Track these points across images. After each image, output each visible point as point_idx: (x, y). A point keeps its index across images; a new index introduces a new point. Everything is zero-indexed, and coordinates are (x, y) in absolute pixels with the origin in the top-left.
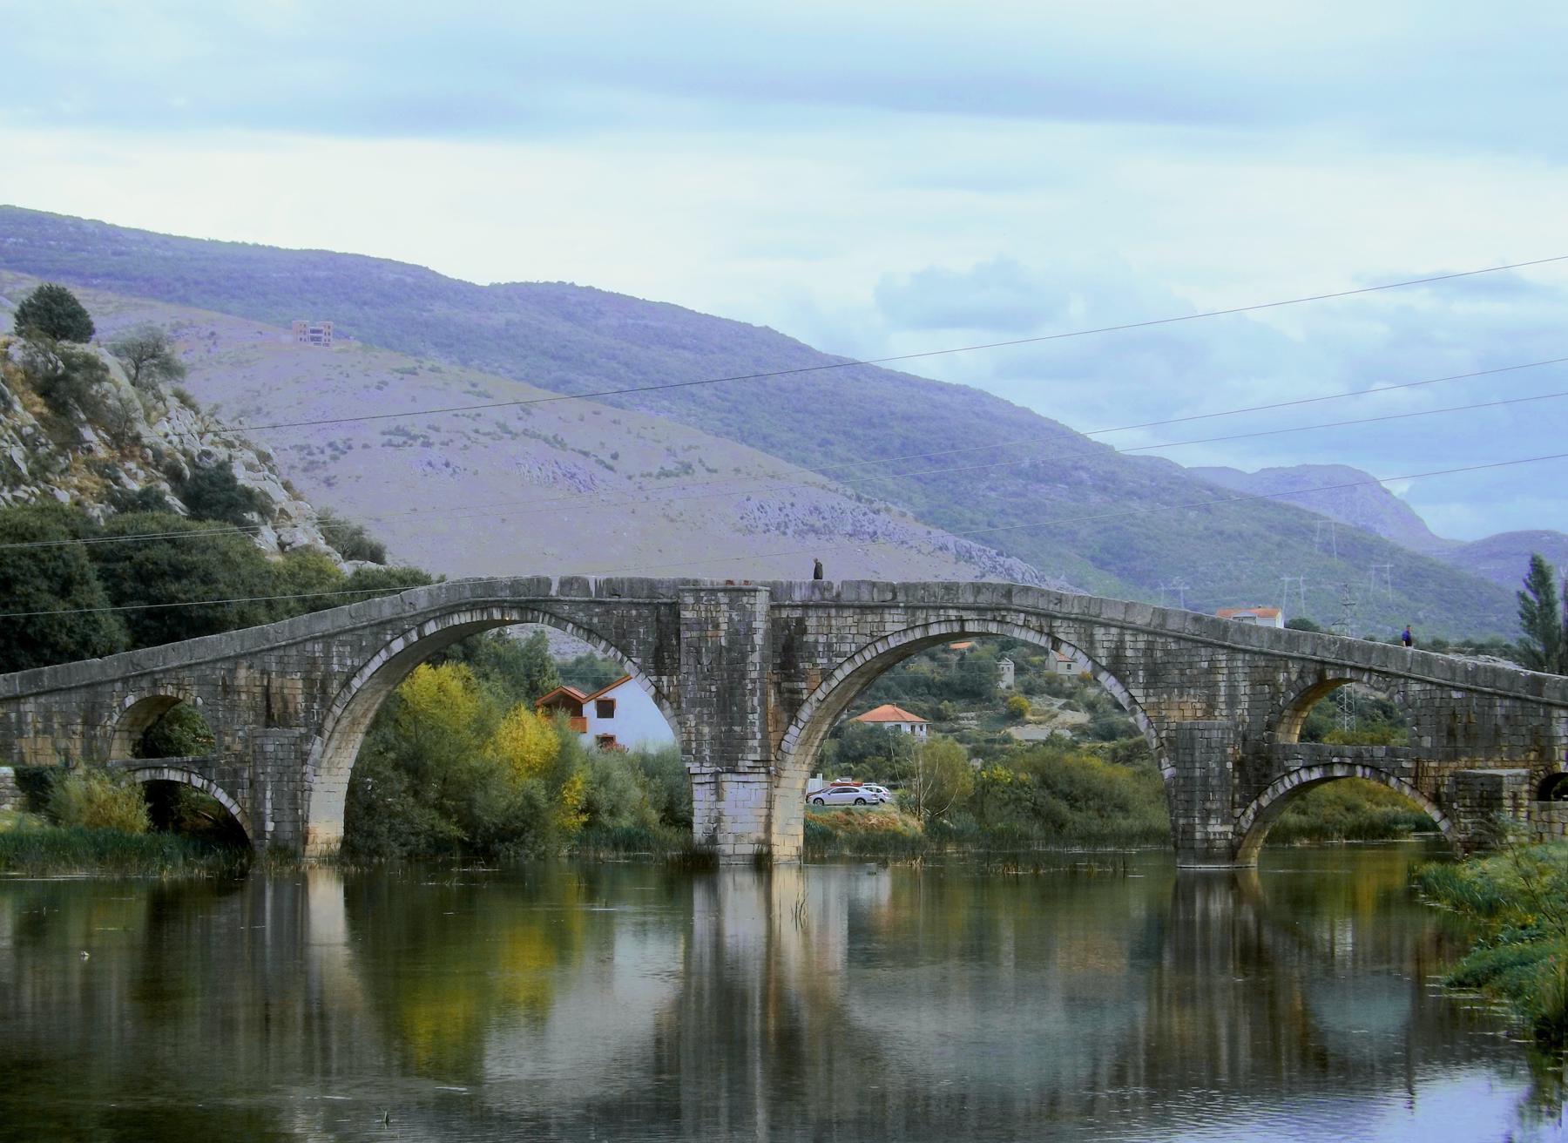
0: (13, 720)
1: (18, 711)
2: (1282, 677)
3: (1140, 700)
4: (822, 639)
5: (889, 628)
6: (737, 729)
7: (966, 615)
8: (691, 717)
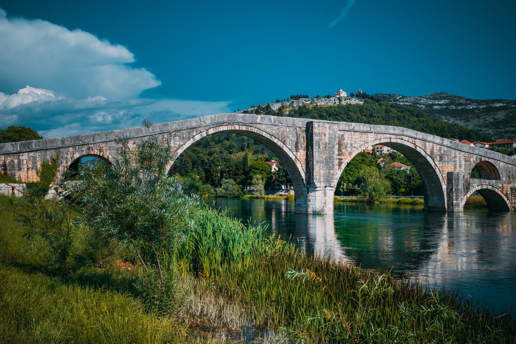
0: (16, 163)
1: (19, 159)
2: (472, 160)
3: (438, 165)
4: (349, 142)
6: (331, 171)
7: (392, 136)
8: (317, 167)
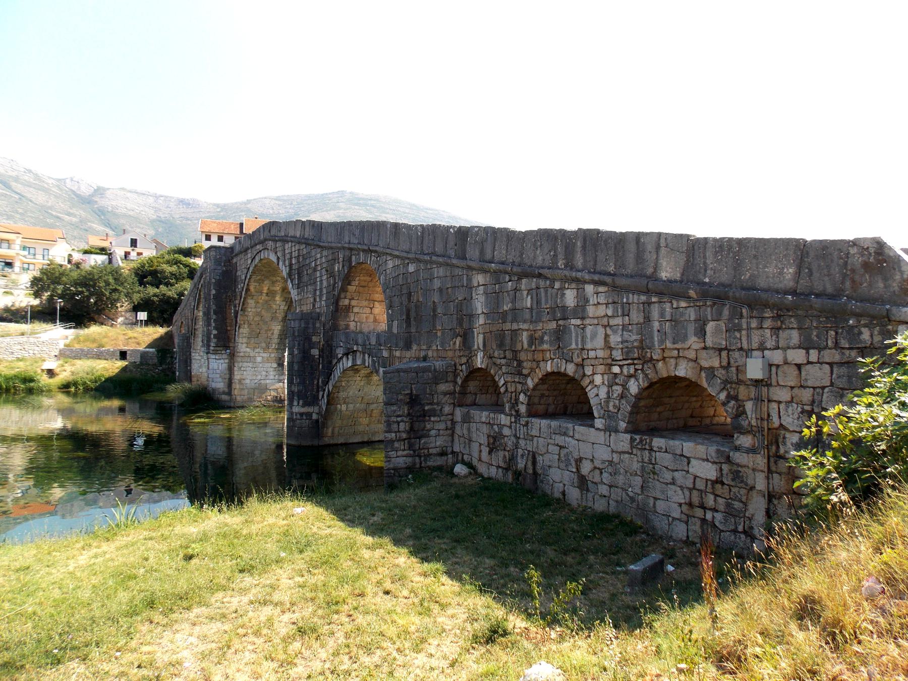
5: (249, 262)
